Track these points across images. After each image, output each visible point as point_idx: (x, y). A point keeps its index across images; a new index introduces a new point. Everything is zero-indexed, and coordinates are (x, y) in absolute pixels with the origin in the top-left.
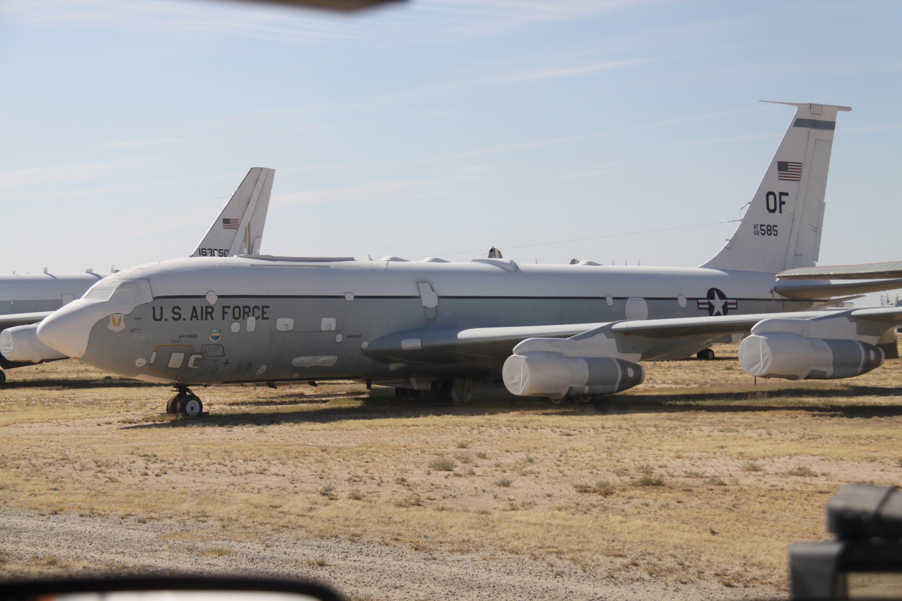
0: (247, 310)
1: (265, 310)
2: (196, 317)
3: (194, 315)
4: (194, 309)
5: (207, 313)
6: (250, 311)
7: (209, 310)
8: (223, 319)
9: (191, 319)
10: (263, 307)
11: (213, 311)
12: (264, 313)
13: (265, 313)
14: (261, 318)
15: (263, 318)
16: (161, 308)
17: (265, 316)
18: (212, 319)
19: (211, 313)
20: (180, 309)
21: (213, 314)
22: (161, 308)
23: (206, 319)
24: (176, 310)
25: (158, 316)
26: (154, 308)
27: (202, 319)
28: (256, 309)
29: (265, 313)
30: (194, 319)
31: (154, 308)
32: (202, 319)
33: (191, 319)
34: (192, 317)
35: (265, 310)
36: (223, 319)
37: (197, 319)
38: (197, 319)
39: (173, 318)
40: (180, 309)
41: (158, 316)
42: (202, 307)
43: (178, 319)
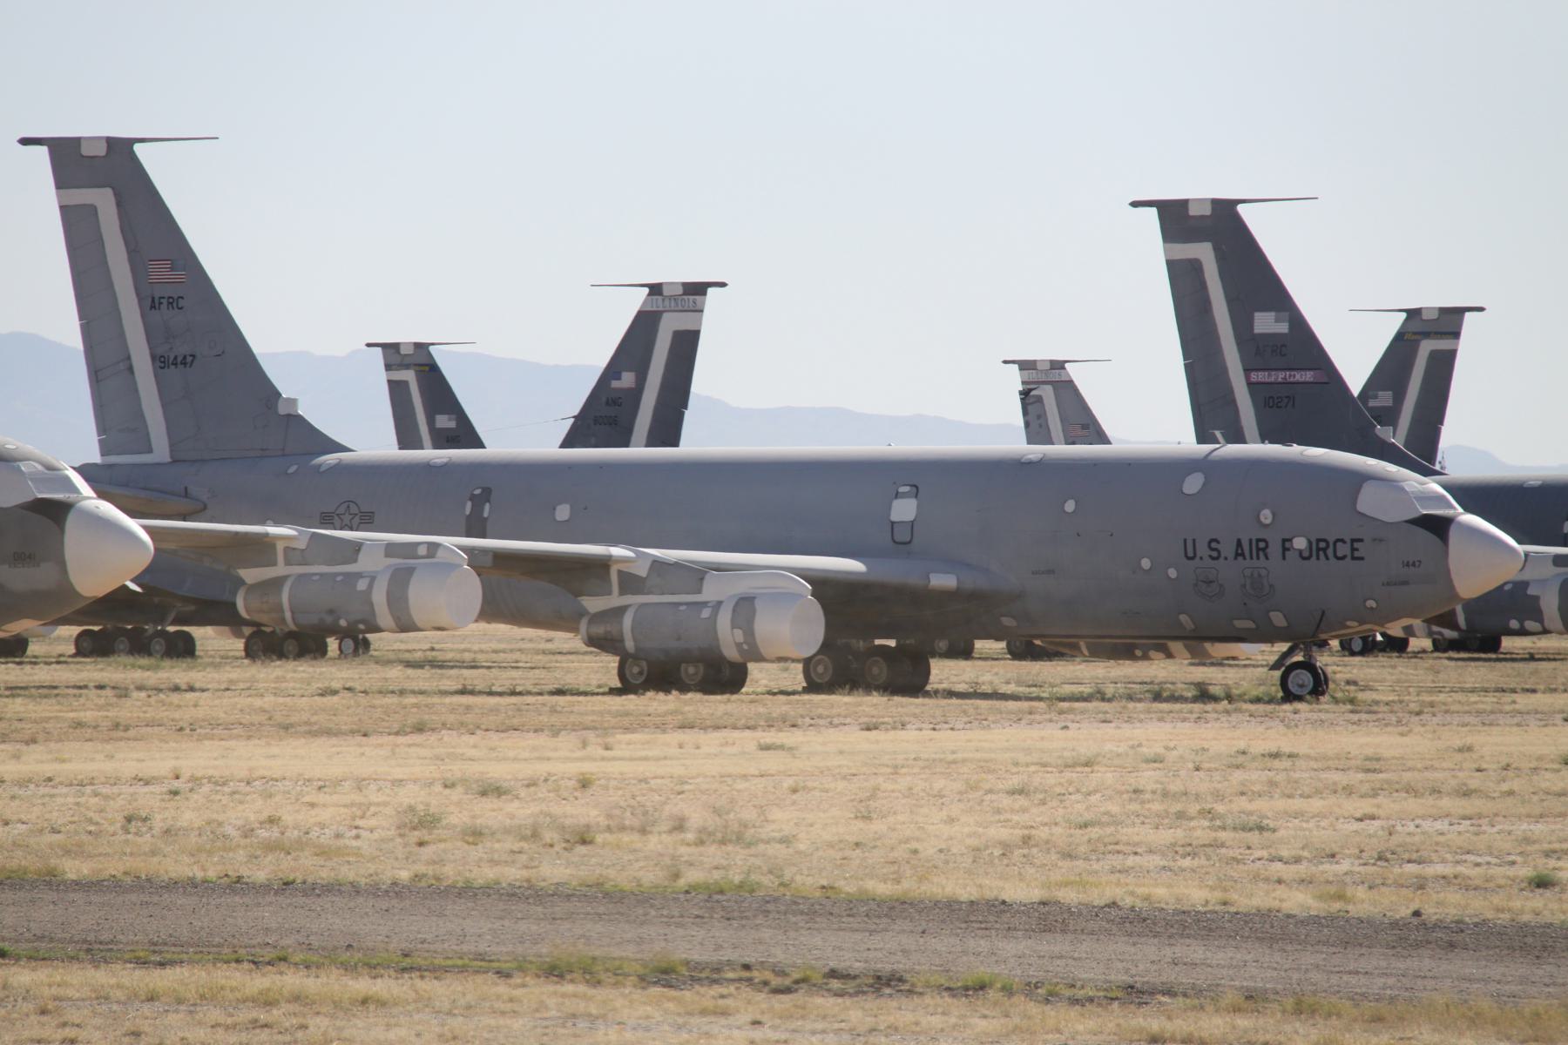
0: (1322, 545)
1: (1356, 545)
2: (1243, 555)
3: (1240, 551)
4: (1239, 543)
5: (1258, 549)
6: (1328, 546)
7: (1262, 545)
8: (1284, 558)
9: (1236, 558)
10: (1353, 541)
11: (1267, 546)
12: (1353, 549)
13: (1357, 550)
14: (1349, 557)
15: (1353, 558)
16: (1194, 540)
17: (1356, 554)
18: (1267, 558)
19: (1264, 550)
20: (1218, 542)
21: (1269, 550)
22: (1194, 540)
23: (1258, 558)
24: (1214, 545)
25: (1190, 554)
26: (1185, 541)
27: (1252, 558)
28: (1339, 545)
29: (1357, 550)
30: (1240, 558)
31: (1185, 541)
32: (1252, 558)
33: (1236, 558)
34: (1237, 555)
35: (1356, 545)
36: (1284, 558)
37: (1245, 559)
38: (1245, 559)
39: (1210, 556)
40: (1218, 542)
41: (1190, 554)
42: (1251, 541)
43: (1217, 558)
